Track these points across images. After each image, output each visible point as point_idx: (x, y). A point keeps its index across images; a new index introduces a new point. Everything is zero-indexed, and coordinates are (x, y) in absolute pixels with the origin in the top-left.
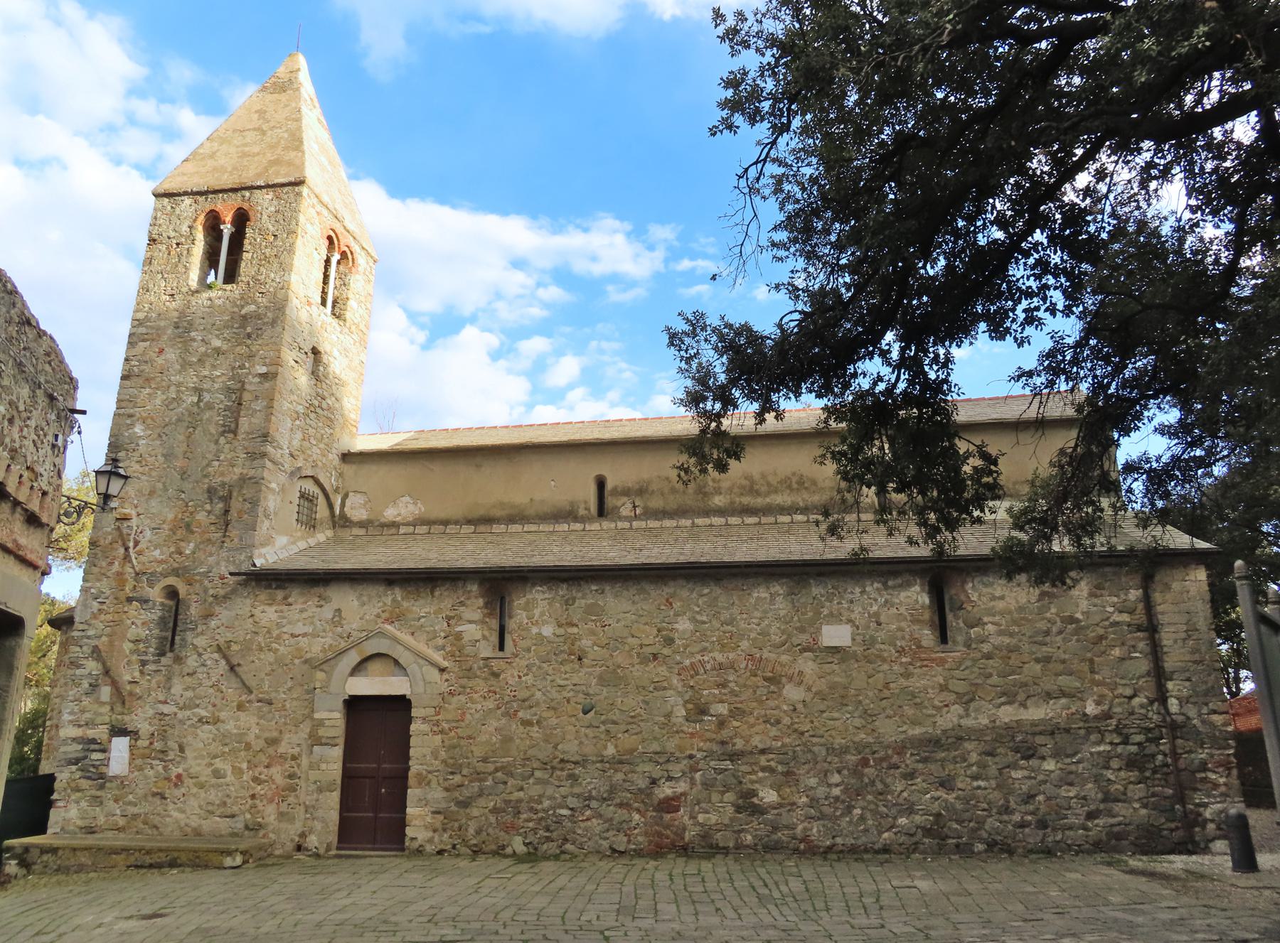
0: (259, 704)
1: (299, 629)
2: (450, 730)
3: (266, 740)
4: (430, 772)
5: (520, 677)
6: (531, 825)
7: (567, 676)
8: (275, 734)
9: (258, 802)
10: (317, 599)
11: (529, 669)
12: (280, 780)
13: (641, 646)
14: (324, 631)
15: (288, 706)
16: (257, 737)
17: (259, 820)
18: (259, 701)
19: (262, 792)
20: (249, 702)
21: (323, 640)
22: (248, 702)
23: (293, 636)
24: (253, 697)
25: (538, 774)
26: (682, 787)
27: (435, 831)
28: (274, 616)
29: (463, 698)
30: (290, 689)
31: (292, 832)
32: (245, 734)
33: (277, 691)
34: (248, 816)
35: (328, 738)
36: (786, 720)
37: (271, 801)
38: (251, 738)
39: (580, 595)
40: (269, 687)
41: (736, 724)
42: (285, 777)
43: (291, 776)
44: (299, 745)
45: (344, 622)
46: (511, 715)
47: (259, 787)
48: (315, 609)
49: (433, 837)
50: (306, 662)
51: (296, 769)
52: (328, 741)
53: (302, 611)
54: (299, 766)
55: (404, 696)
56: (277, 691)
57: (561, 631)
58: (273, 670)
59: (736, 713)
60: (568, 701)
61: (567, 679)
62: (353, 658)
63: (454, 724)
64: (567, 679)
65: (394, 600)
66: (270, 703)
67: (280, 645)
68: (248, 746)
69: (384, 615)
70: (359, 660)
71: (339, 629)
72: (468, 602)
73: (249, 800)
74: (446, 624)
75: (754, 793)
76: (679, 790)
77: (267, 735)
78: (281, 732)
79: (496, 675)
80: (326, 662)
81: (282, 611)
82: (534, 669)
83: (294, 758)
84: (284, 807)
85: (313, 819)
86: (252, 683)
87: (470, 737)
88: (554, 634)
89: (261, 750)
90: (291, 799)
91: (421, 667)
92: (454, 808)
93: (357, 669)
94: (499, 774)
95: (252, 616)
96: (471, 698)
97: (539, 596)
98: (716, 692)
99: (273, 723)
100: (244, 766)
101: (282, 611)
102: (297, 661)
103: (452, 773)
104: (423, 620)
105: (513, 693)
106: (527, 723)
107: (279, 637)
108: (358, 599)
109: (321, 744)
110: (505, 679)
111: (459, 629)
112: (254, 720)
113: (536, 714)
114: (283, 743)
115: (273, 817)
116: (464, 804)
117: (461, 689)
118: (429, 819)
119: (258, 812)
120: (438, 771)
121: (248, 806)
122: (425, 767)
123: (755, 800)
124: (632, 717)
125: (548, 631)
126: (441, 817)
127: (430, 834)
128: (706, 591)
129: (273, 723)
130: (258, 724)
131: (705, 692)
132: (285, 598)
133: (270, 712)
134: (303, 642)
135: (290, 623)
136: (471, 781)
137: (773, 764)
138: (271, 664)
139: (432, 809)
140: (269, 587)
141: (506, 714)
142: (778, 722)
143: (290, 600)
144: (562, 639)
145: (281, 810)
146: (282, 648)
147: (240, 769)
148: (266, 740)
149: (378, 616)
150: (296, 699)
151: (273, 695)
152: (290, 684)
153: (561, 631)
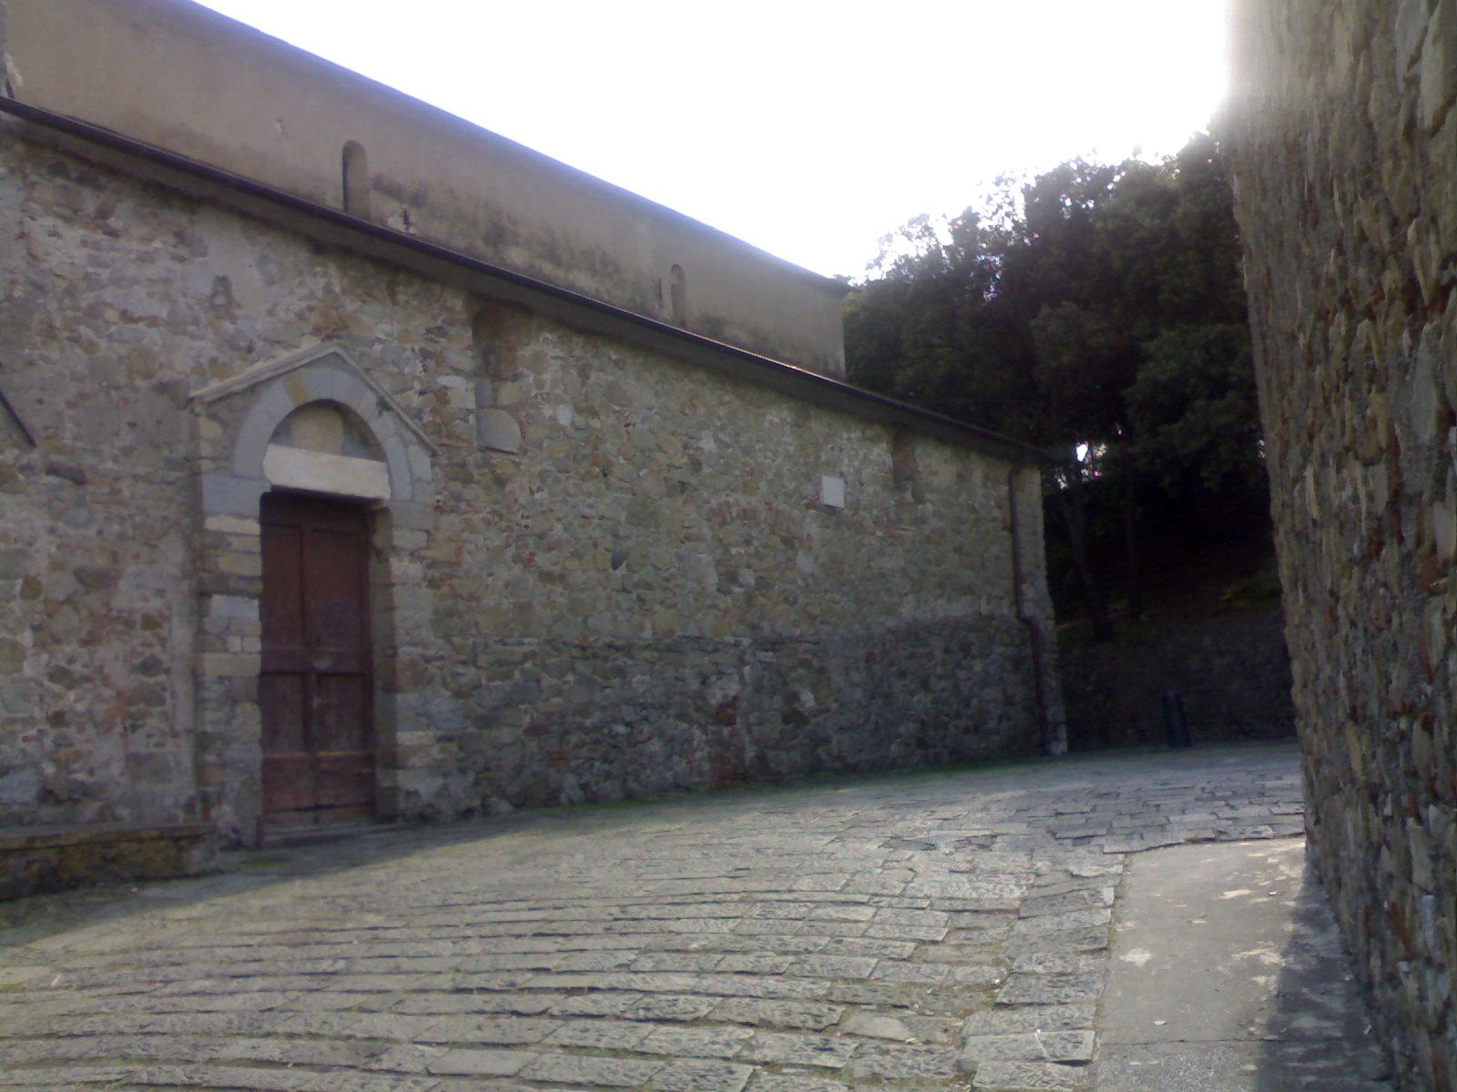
0: (51, 479)
1: (141, 302)
2: (442, 580)
3: (80, 575)
4: (428, 660)
5: (532, 493)
6: (584, 752)
7: (590, 501)
8: (101, 561)
9: (71, 731)
10: (173, 240)
11: (543, 481)
12: (124, 678)
13: (671, 467)
14: (196, 321)
15: (126, 494)
16: (57, 566)
17: (80, 776)
18: (53, 470)
19: (80, 707)
20: (27, 469)
21: (197, 344)
22: (23, 469)
23: (126, 316)
24: (34, 456)
25: (580, 666)
26: (733, 688)
27: (445, 775)
28: (80, 255)
29: (455, 519)
30: (127, 451)
31: (169, 801)
32: (20, 553)
33: (97, 453)
34: (49, 769)
35: (241, 578)
36: (802, 600)
37: (105, 728)
38: (39, 565)
39: (596, 363)
40: (76, 438)
41: (762, 600)
42: (134, 670)
43: (149, 667)
44: (160, 592)
45: (240, 312)
46: (528, 562)
47: (72, 695)
48: (170, 264)
49: (445, 787)
50: (163, 388)
51: (158, 650)
52: (242, 585)
53: (144, 259)
54: (163, 641)
55: (376, 501)
56: (97, 453)
57: (580, 421)
58: (83, 396)
59: (763, 584)
60: (596, 545)
61: (591, 506)
62: (278, 402)
63: (446, 570)
64: (591, 506)
65: (328, 290)
66: (79, 479)
67: (97, 330)
68: (32, 588)
69: (315, 318)
70: (291, 407)
71: (228, 327)
72: (453, 331)
73: (46, 727)
74: (419, 368)
75: (793, 697)
76: (732, 693)
77: (77, 561)
78: (114, 556)
79: (501, 482)
80: (228, 407)
81: (97, 246)
82: (550, 481)
83: (151, 622)
84: (139, 744)
85: (223, 765)
86: (34, 421)
87: (472, 597)
88: (573, 424)
89: (69, 600)
90: (154, 723)
91: (406, 444)
92: (472, 729)
93: (282, 433)
94: (528, 665)
95: (22, 236)
96: (468, 521)
97: (551, 351)
98: (742, 550)
99: (92, 532)
100: (27, 638)
101: (97, 246)
102: (141, 383)
103: (464, 663)
104: (378, 347)
105: (524, 522)
106: (546, 577)
107: (93, 312)
108: (263, 260)
109: (230, 592)
110: (512, 492)
111: (443, 381)
112: (40, 521)
113: (556, 563)
114: (123, 585)
115: (116, 769)
116: (486, 722)
117: (453, 503)
118: (436, 753)
119: (78, 755)
120: (442, 658)
121: (48, 743)
122: (420, 650)
123: (796, 705)
124: (667, 580)
125: (565, 416)
126: (453, 747)
127: (439, 781)
128: (727, 398)
129: (92, 532)
130: (52, 531)
131: (734, 551)
132: (103, 214)
133: (81, 502)
134: (153, 336)
135: (117, 281)
136: (491, 679)
137: (809, 656)
138: (79, 379)
139: (441, 733)
140: (57, 170)
141: (516, 559)
142: (796, 601)
143: (113, 222)
144: (581, 435)
145: (133, 749)
146: (103, 344)
147: (15, 646)
148: (80, 575)
149: (301, 316)
150: (147, 478)
151: (88, 460)
152: (127, 438)
153: (580, 421)
